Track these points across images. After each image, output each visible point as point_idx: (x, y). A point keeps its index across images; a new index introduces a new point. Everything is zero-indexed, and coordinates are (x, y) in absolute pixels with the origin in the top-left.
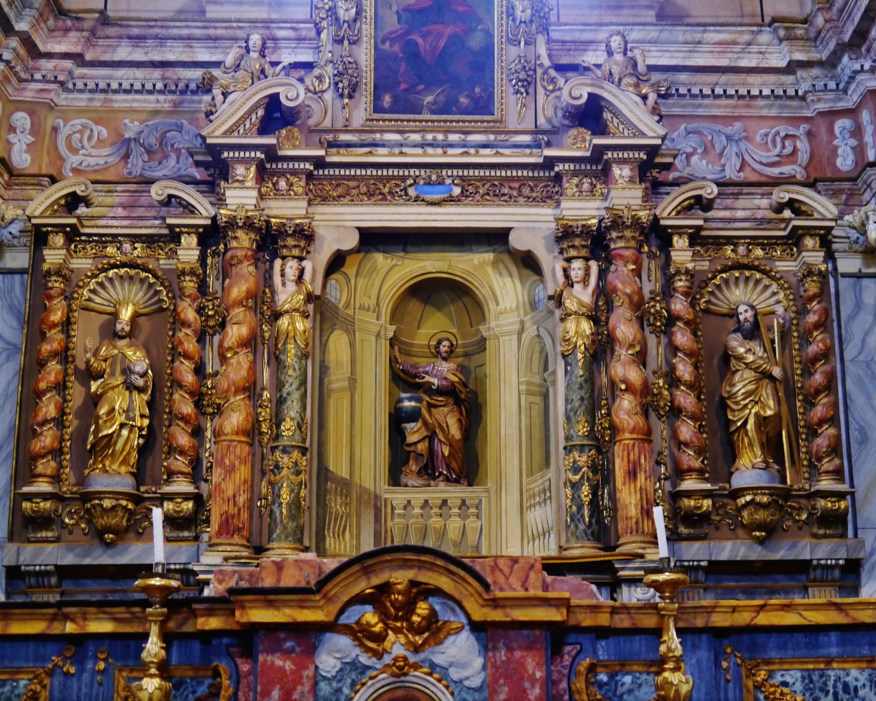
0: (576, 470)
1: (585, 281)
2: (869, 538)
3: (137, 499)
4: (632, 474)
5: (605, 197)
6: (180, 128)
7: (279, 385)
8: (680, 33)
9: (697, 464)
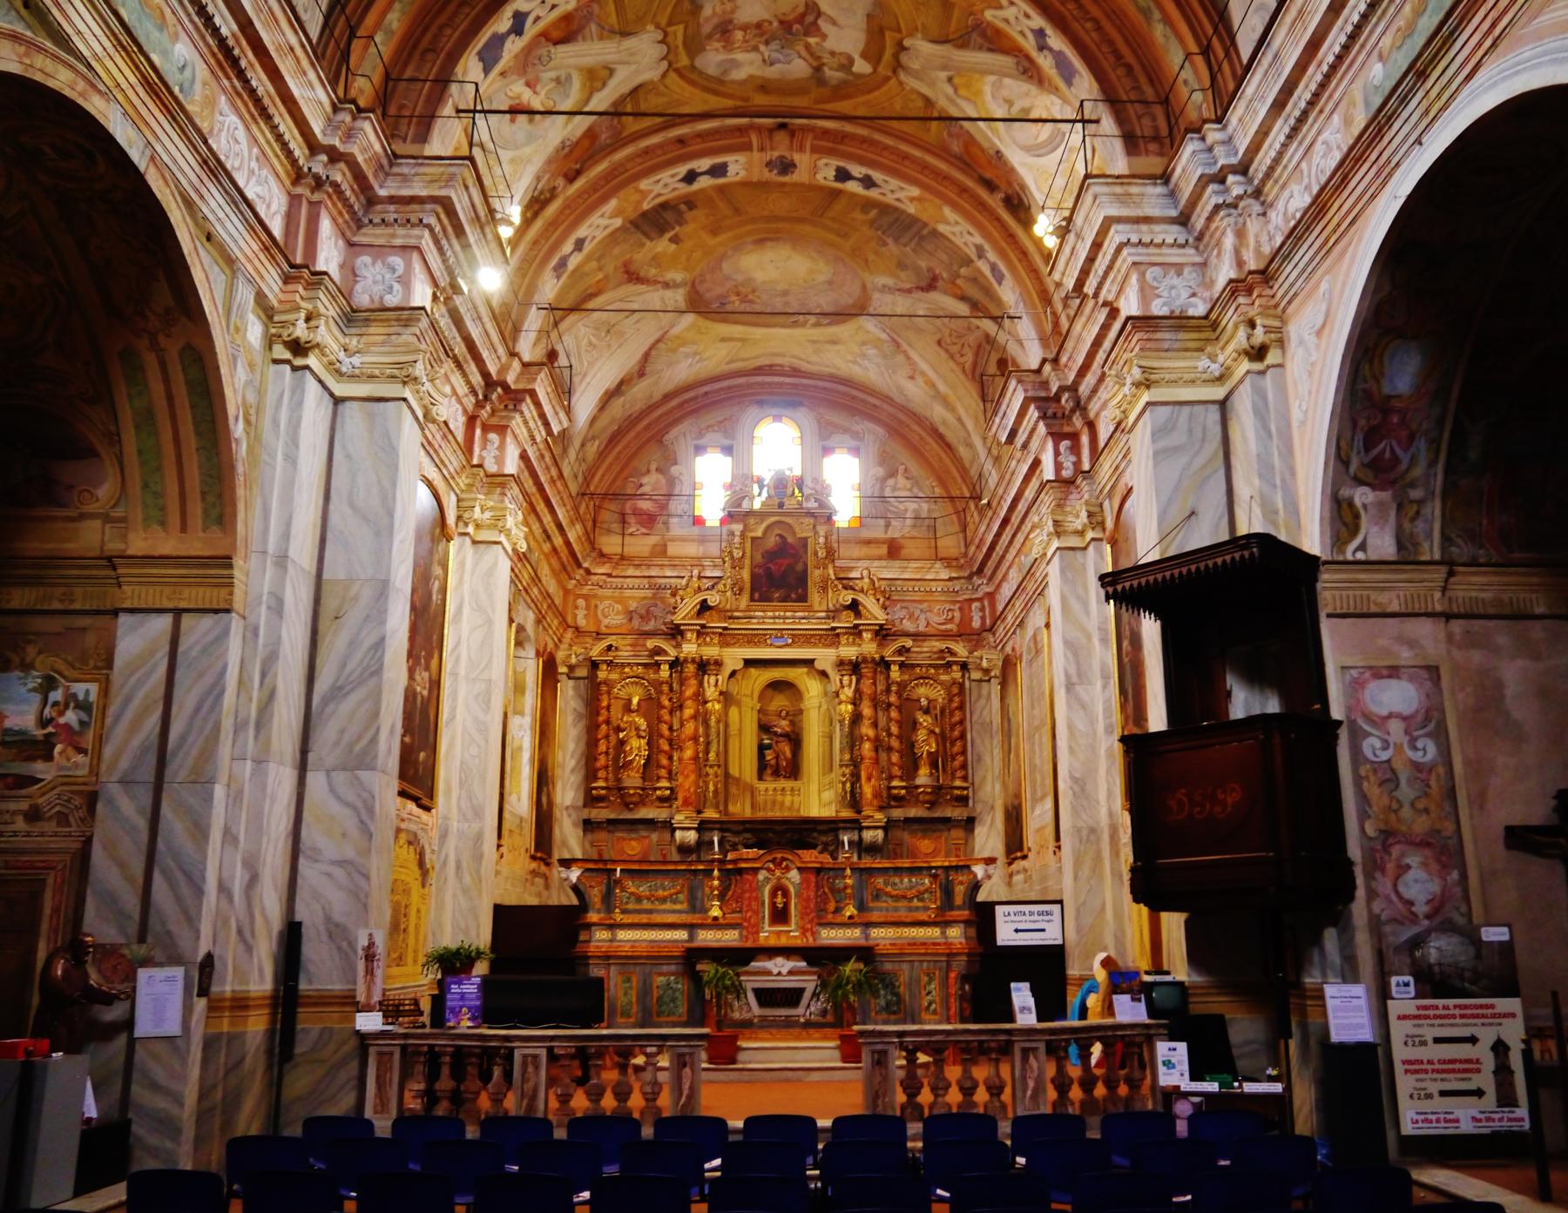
0: (844, 775)
1: (850, 685)
2: (979, 808)
3: (643, 789)
4: (869, 779)
5: (860, 645)
6: (656, 606)
7: (707, 735)
8: (897, 563)
9: (899, 774)
